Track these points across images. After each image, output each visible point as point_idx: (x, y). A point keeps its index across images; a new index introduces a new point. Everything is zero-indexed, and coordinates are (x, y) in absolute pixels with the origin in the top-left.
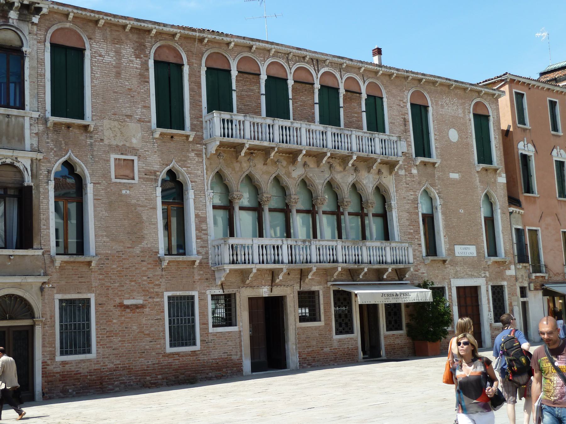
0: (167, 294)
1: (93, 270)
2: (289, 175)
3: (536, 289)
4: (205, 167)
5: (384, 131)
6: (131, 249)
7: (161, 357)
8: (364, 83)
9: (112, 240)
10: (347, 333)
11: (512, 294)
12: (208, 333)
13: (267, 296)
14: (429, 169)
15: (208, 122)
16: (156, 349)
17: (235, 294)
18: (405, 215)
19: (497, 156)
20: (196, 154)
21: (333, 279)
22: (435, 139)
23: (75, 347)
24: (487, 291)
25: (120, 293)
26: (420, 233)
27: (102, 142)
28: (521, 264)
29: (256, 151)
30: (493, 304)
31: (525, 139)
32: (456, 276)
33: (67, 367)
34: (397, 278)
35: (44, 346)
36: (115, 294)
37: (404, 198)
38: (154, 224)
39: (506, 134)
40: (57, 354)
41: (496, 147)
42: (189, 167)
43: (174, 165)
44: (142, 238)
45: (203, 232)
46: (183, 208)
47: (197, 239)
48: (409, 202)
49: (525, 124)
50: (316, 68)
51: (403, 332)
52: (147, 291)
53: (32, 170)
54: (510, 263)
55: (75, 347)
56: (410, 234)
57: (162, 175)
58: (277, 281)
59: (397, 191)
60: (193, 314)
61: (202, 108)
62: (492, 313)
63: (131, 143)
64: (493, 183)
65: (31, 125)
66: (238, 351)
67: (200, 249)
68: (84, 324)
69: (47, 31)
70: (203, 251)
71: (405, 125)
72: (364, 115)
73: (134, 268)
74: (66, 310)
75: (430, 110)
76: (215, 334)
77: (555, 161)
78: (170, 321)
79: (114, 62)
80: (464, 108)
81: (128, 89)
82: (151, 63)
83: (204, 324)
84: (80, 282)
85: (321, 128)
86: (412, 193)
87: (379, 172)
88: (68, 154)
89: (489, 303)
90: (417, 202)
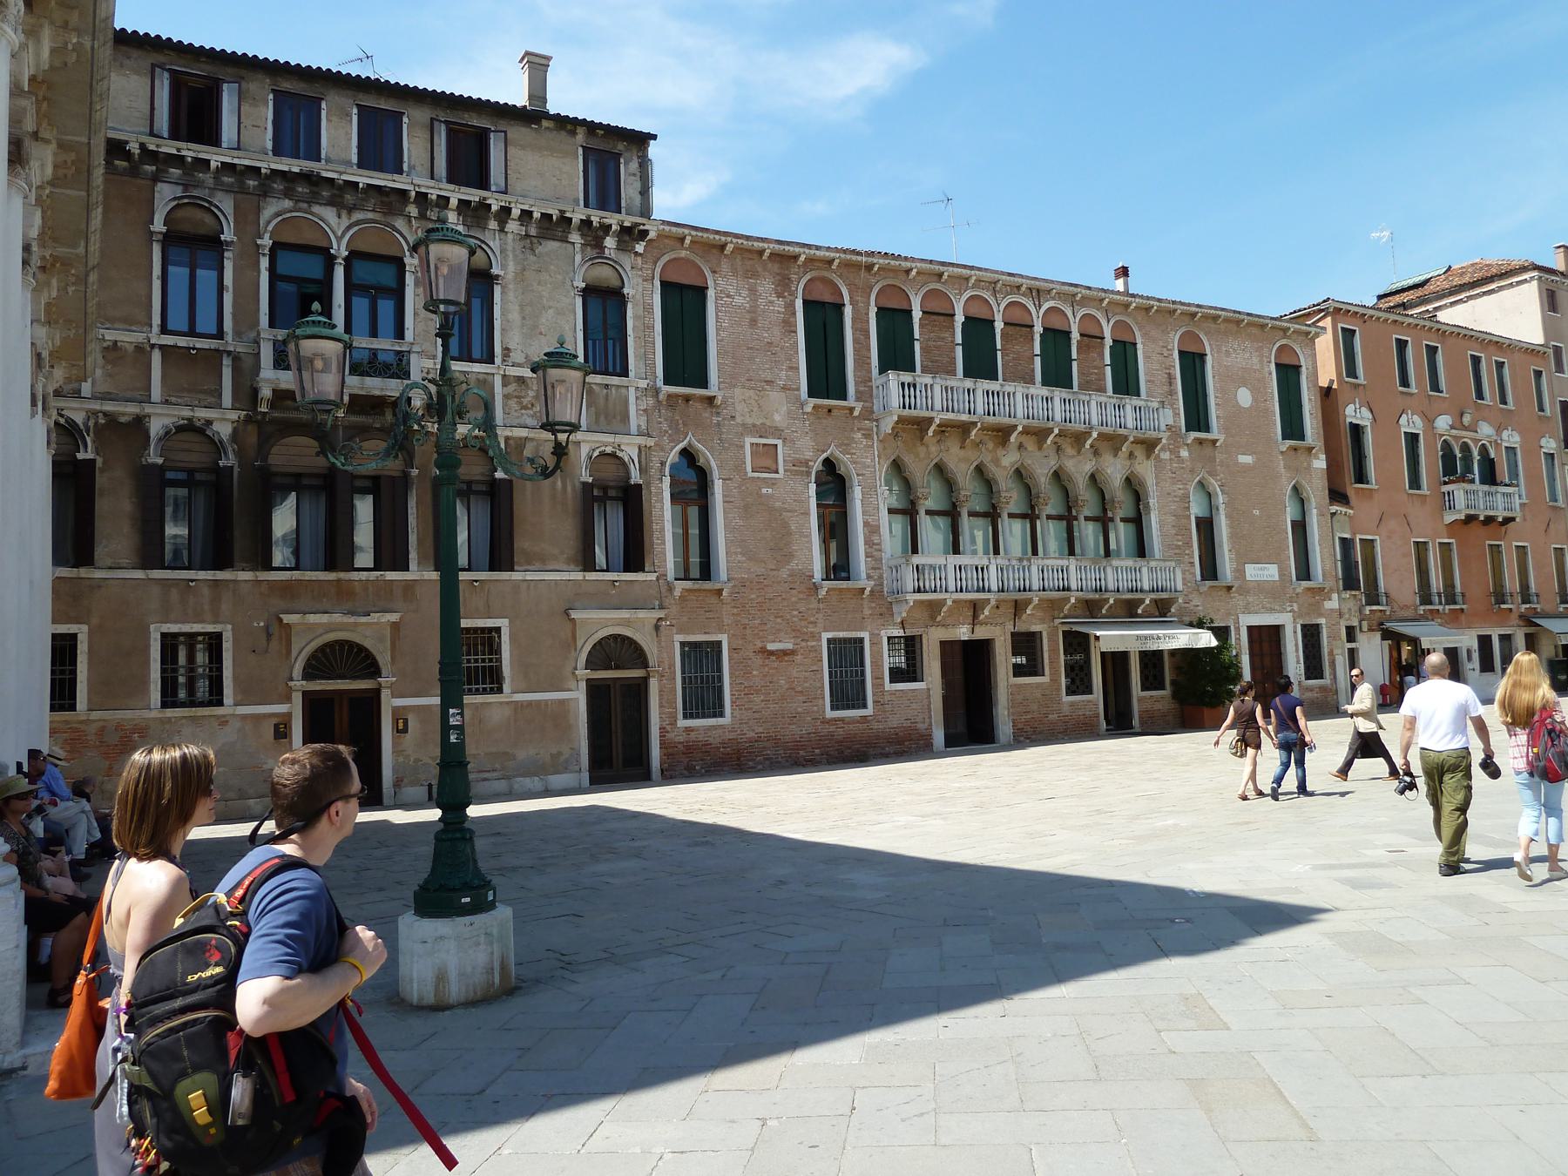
0: (826, 636)
1: (725, 601)
2: (997, 462)
3: (1371, 630)
4: (876, 453)
5: (1138, 395)
6: (775, 573)
7: (819, 723)
8: (1108, 322)
9: (750, 559)
10: (1083, 693)
11: (1333, 637)
12: (883, 692)
14: (1208, 450)
15: (881, 387)
16: (813, 712)
17: (921, 636)
18: (1171, 519)
19: (1312, 428)
20: (863, 434)
21: (1062, 615)
22: (1216, 404)
23: (703, 708)
24: (1295, 632)
25: (761, 633)
26: (1192, 546)
27: (734, 421)
28: (1348, 592)
29: (949, 429)
30: (1304, 652)
31: (1357, 400)
32: (1248, 610)
33: (693, 735)
34: (1157, 614)
35: (661, 706)
36: (755, 635)
37: (1169, 494)
38: (807, 536)
39: (1327, 393)
40: (678, 716)
41: (1311, 414)
42: (855, 454)
43: (832, 451)
44: (790, 556)
46: (846, 512)
47: (867, 557)
48: (1175, 499)
49: (1357, 378)
50: (1037, 303)
51: (1166, 693)
52: (799, 630)
53: (640, 462)
54: (1331, 590)
55: (703, 708)
56: (1178, 547)
57: (817, 465)
58: (982, 617)
60: (862, 664)
61: (871, 368)
62: (1302, 666)
63: (773, 420)
64: (1306, 469)
65: (637, 398)
66: (926, 717)
67: (870, 572)
68: (713, 677)
69: (655, 263)
70: (875, 574)
71: (1170, 384)
72: (1108, 369)
73: (780, 598)
74: (689, 657)
75: (1209, 359)
76: (893, 693)
77: (1405, 433)
78: (830, 673)
79: (748, 305)
80: (1261, 356)
81: (768, 343)
82: (799, 304)
83: (878, 678)
84: (707, 618)
85: (1045, 391)
86: (1181, 487)
87: (1131, 455)
88: (688, 438)
89: (1297, 650)
90: (1188, 500)
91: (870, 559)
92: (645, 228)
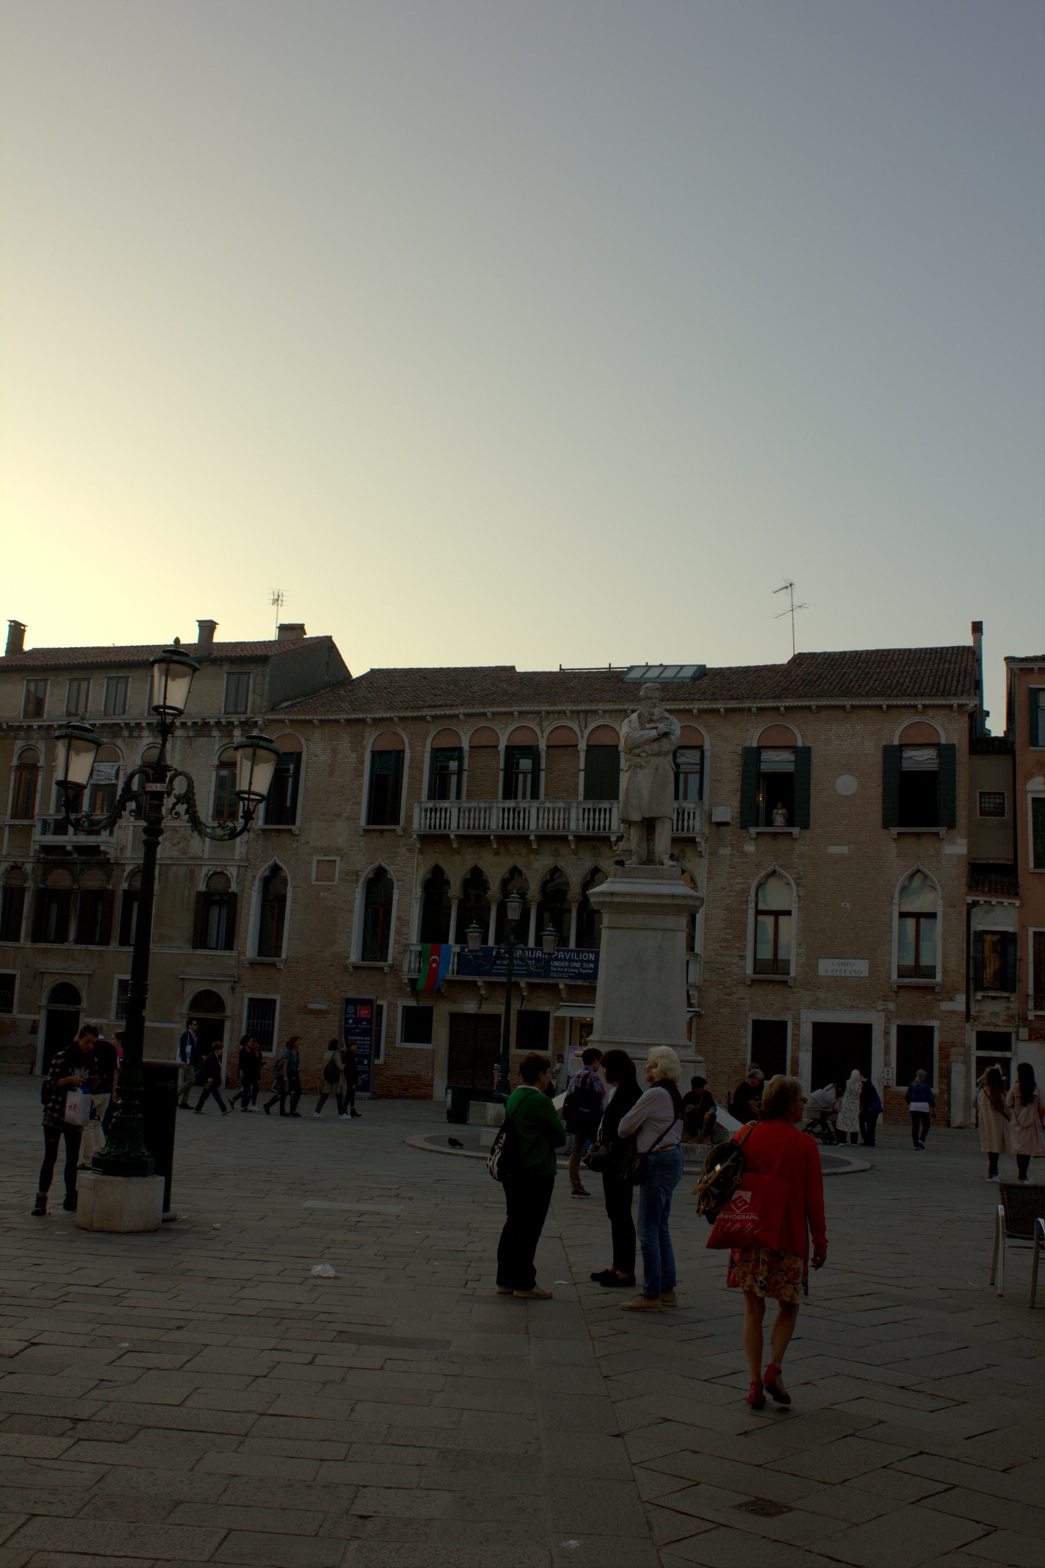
13: (473, 1012)
20: (408, 849)
42: (396, 865)
43: (380, 861)
45: (403, 936)
47: (395, 944)
48: (731, 894)
53: (238, 877)
59: (709, 879)
81: (341, 786)
82: (368, 757)
86: (741, 881)
91: (397, 946)
92: (256, 719)
